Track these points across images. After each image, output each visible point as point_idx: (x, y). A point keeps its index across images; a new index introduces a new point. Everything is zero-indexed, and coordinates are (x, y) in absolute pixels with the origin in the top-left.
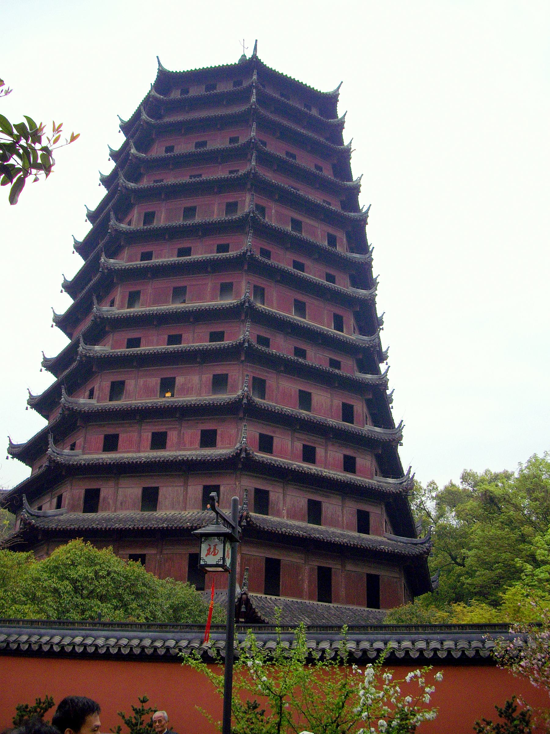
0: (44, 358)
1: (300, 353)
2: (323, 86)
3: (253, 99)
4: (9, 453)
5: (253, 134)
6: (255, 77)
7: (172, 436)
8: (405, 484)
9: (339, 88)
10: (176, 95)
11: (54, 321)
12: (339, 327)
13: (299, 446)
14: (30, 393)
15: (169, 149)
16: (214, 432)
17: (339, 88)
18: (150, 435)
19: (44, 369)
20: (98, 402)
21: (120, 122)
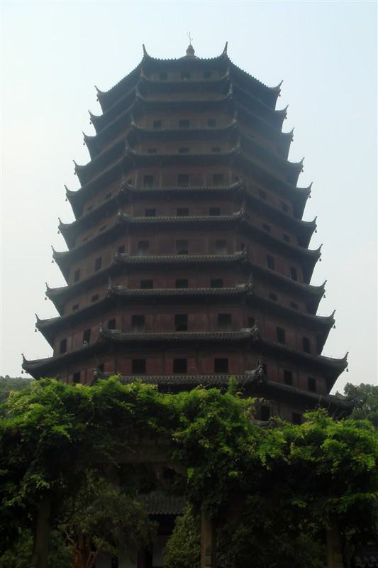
0: (48, 288)
1: (273, 297)
2: (269, 83)
3: (231, 92)
4: (24, 368)
5: (234, 121)
6: (228, 74)
7: (191, 364)
8: (353, 401)
9: (280, 85)
10: (154, 78)
11: (54, 257)
12: (295, 278)
13: (282, 371)
14: (37, 318)
15: (157, 124)
16: (226, 361)
17: (280, 85)
18: (172, 361)
19: (48, 298)
20: (123, 331)
21: (97, 92)
